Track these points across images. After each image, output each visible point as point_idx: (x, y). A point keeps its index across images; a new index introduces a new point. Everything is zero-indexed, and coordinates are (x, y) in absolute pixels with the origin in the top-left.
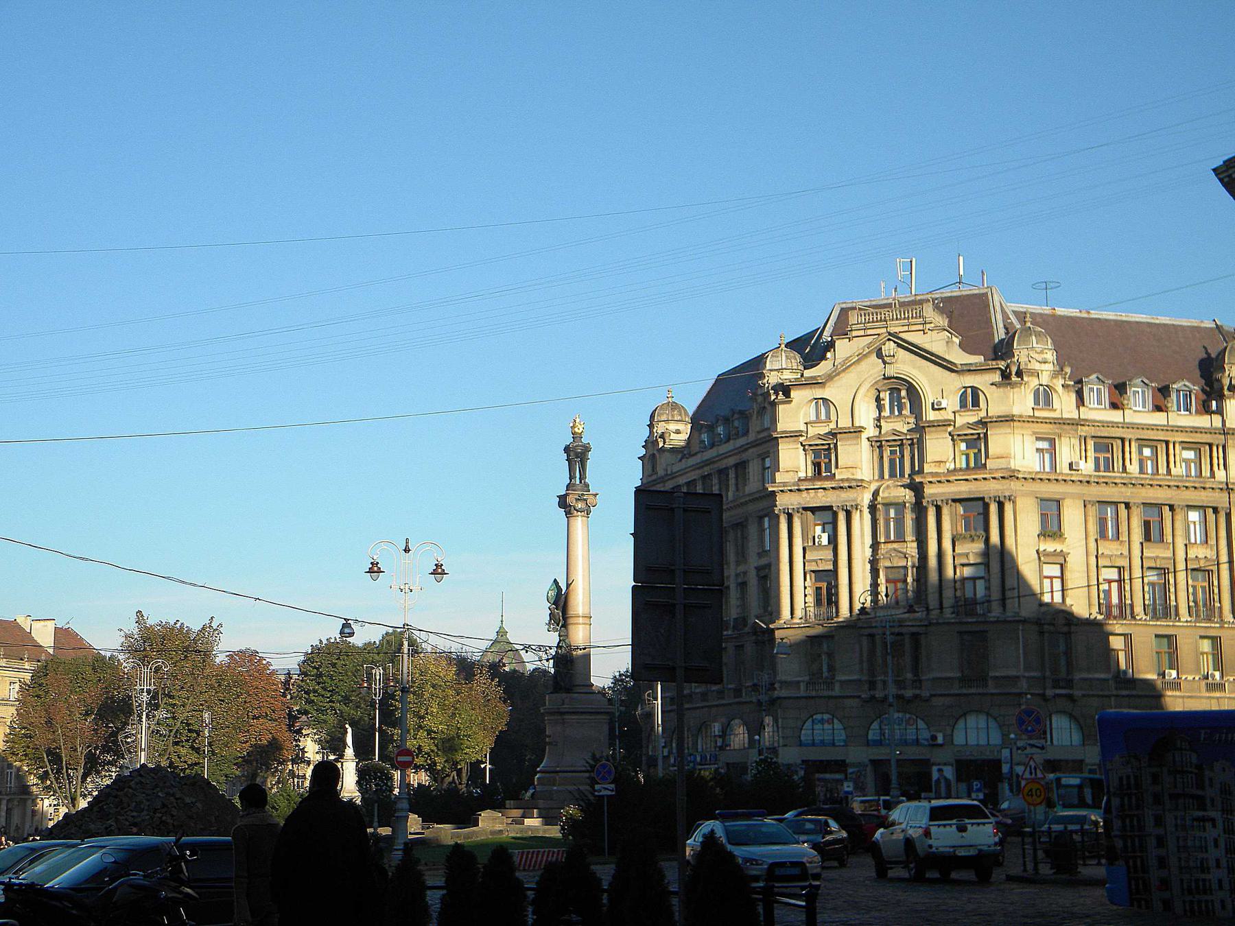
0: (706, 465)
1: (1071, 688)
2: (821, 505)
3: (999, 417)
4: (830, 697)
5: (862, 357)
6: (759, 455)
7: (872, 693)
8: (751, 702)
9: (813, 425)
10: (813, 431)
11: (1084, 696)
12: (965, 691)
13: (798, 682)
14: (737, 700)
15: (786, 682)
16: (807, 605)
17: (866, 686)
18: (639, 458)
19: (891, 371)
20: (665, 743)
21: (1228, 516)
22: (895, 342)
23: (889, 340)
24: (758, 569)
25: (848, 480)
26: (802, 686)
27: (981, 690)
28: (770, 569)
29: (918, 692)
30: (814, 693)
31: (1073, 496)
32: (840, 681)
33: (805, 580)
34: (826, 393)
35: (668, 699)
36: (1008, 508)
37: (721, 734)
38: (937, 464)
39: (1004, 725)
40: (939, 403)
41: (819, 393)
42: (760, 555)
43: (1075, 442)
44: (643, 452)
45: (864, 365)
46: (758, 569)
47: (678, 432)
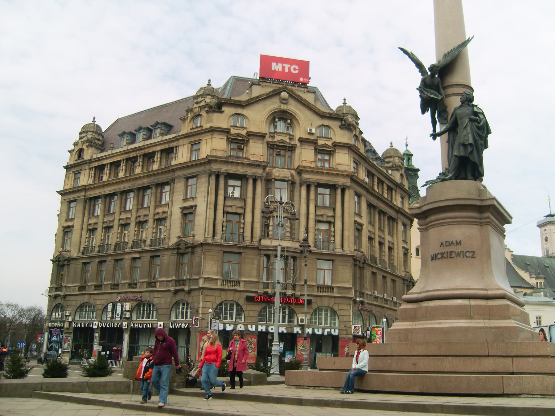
0: (134, 151)
1: (363, 297)
2: (239, 173)
3: (344, 143)
4: (236, 291)
5: (269, 96)
6: (190, 142)
7: (267, 290)
8: (169, 291)
9: (235, 128)
10: (233, 131)
11: (368, 303)
12: (321, 294)
13: (217, 279)
14: (150, 289)
15: (208, 278)
16: (223, 232)
17: (261, 286)
18: (68, 151)
19: (284, 107)
20: (70, 314)
21: (397, 223)
22: (287, 93)
23: (285, 91)
24: (183, 209)
25: (257, 161)
26: (219, 282)
27: (329, 294)
28: (195, 208)
29: (293, 292)
30: (226, 287)
31: (366, 197)
32: (245, 281)
33: (223, 217)
34: (245, 112)
35: (77, 288)
36: (347, 192)
37: (130, 310)
38: (310, 162)
39: (341, 315)
40: (311, 130)
41: (240, 111)
42: (185, 200)
43: (364, 168)
44: (72, 147)
45: (268, 102)
46: (183, 209)
47: (99, 140)
